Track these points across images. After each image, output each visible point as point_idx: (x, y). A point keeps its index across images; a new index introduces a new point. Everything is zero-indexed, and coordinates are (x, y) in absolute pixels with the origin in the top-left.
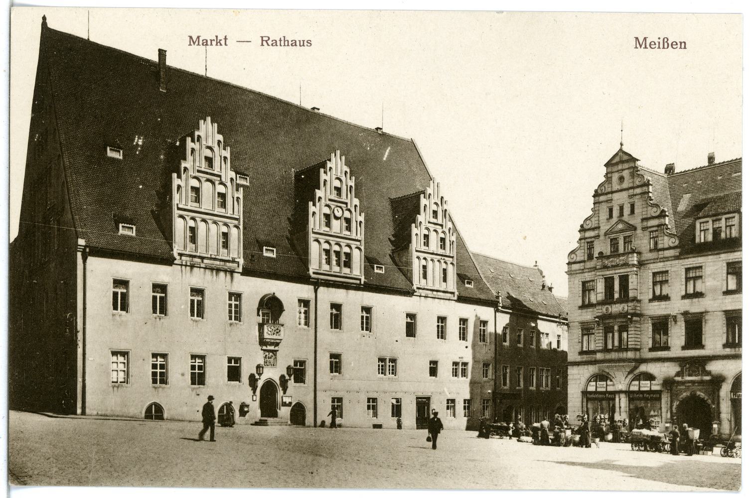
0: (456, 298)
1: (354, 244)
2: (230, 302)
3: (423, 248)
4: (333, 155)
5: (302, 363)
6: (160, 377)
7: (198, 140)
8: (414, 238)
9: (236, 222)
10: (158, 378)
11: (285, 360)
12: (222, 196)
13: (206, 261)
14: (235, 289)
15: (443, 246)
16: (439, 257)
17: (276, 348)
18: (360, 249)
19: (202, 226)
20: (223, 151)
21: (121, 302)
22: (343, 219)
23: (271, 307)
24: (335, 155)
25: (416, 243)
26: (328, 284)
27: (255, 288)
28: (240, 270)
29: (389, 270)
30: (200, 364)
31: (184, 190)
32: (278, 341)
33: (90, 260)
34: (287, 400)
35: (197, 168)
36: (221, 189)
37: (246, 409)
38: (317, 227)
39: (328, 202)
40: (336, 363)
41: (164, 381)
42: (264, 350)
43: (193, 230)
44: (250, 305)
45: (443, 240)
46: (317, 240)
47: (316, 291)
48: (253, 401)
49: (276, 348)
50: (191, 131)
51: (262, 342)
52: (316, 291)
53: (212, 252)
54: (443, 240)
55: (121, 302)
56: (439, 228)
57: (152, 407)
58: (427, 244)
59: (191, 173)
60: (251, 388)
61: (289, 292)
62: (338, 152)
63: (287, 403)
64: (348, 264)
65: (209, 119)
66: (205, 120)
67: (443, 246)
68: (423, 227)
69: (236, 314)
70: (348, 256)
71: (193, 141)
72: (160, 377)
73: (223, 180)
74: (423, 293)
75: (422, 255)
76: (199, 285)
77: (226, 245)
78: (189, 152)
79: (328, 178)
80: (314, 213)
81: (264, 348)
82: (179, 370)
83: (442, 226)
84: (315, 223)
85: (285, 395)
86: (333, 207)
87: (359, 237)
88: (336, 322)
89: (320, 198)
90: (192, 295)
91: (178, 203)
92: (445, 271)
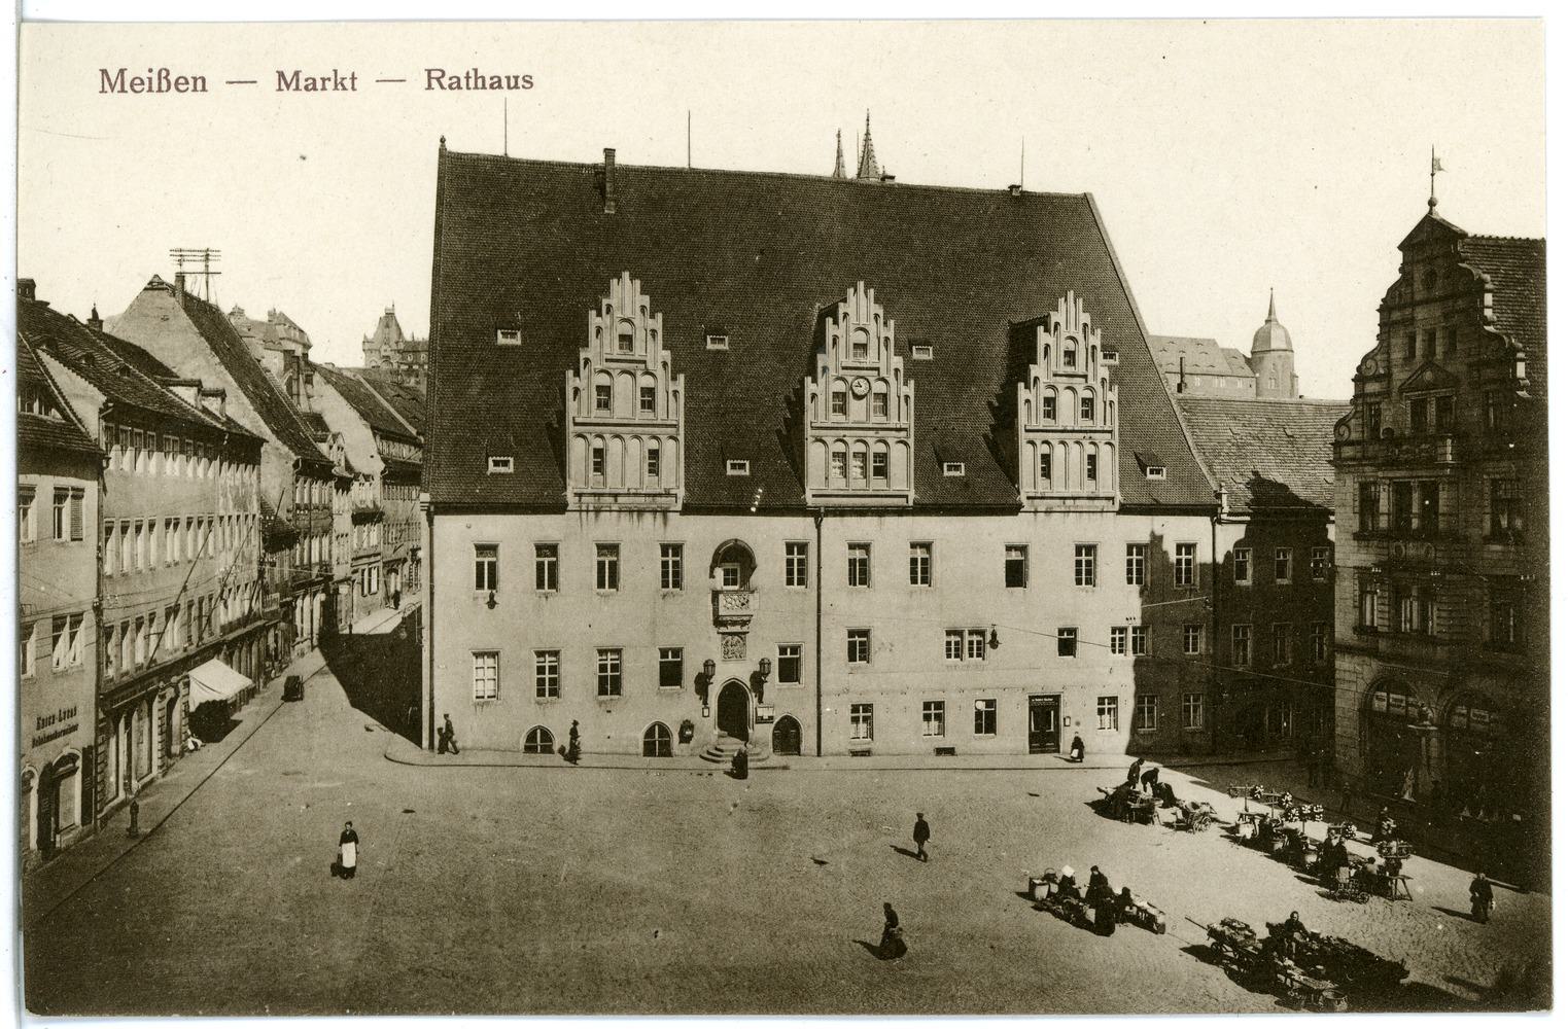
0: (1117, 507)
1: (891, 438)
2: (665, 559)
3: (1044, 423)
4: (851, 291)
5: (795, 650)
6: (549, 685)
7: (608, 312)
8: (1022, 409)
9: (671, 431)
10: (547, 687)
11: (763, 647)
12: (649, 392)
13: (620, 499)
14: (672, 537)
15: (1088, 414)
16: (1080, 436)
17: (745, 629)
18: (906, 444)
19: (614, 446)
20: (650, 321)
21: (487, 577)
22: (871, 398)
23: (736, 560)
24: (856, 291)
25: (1028, 416)
26: (840, 512)
27: (704, 534)
28: (679, 507)
29: (974, 468)
30: (614, 662)
31: (584, 394)
32: (745, 618)
33: (437, 519)
34: (764, 713)
35: (606, 356)
36: (646, 381)
37: (688, 733)
38: (821, 418)
39: (842, 373)
40: (859, 646)
41: (554, 692)
42: (723, 634)
43: (599, 453)
44: (696, 564)
45: (1088, 403)
46: (819, 440)
47: (818, 527)
48: (704, 716)
49: (745, 629)
51: (718, 622)
52: (818, 527)
53: (632, 483)
54: (1088, 403)
55: (487, 577)
56: (1079, 383)
57: (536, 734)
58: (1051, 413)
59: (596, 365)
60: (698, 697)
61: (767, 535)
63: (766, 717)
64: (881, 471)
65: (626, 275)
66: (619, 278)
67: (1088, 414)
68: (1041, 385)
69: (672, 576)
70: (882, 458)
71: (599, 314)
72: (549, 685)
73: (650, 367)
74: (1042, 505)
75: (1038, 437)
76: (610, 537)
77: (654, 469)
78: (592, 331)
79: (840, 332)
80: (814, 396)
81: (723, 629)
82: (580, 674)
83: (1085, 377)
84: (817, 412)
85: (761, 705)
86: (850, 379)
87: (903, 423)
88: (859, 573)
89: (825, 369)
91: (576, 414)
92: (1092, 459)
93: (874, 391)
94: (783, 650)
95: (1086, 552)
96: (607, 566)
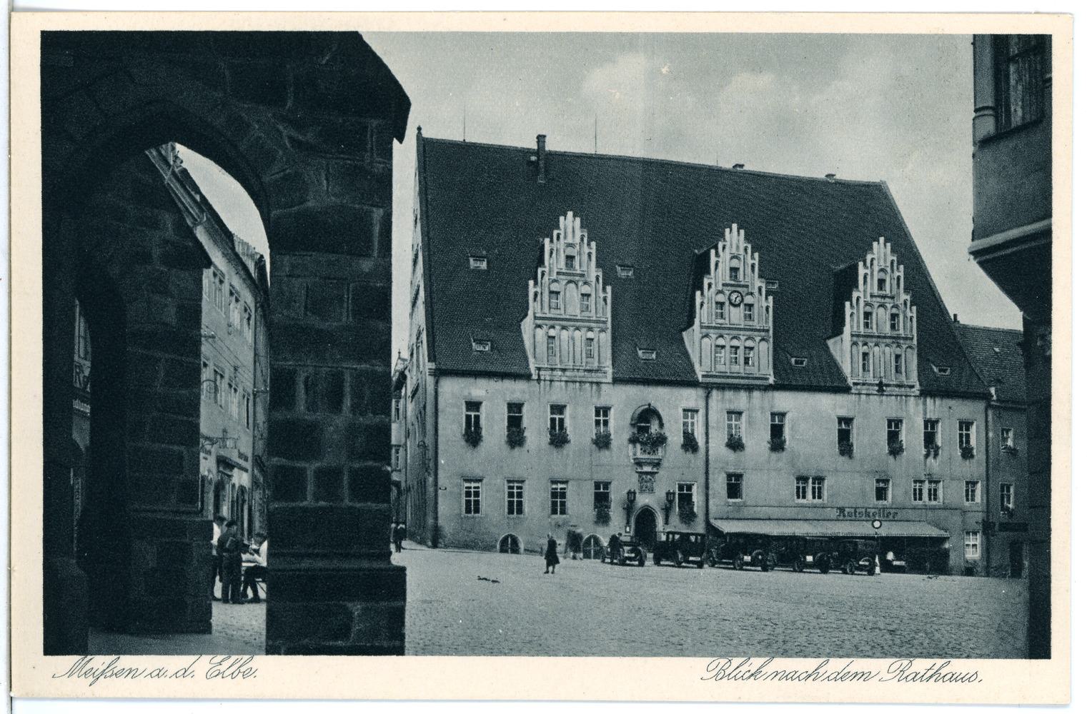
4: (727, 230)
13: (568, 373)
14: (602, 402)
24: (731, 231)
26: (722, 387)
28: (609, 379)
41: (520, 511)
42: (641, 472)
47: (707, 398)
50: (549, 227)
52: (707, 398)
62: (735, 226)
82: (535, 499)
89: (710, 285)
90: (552, 413)
93: (745, 302)
94: (681, 487)
95: (894, 427)
96: (557, 422)
